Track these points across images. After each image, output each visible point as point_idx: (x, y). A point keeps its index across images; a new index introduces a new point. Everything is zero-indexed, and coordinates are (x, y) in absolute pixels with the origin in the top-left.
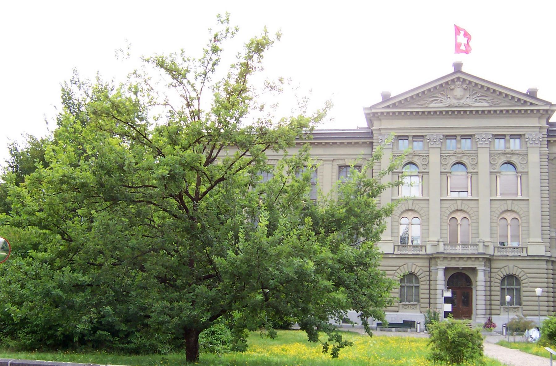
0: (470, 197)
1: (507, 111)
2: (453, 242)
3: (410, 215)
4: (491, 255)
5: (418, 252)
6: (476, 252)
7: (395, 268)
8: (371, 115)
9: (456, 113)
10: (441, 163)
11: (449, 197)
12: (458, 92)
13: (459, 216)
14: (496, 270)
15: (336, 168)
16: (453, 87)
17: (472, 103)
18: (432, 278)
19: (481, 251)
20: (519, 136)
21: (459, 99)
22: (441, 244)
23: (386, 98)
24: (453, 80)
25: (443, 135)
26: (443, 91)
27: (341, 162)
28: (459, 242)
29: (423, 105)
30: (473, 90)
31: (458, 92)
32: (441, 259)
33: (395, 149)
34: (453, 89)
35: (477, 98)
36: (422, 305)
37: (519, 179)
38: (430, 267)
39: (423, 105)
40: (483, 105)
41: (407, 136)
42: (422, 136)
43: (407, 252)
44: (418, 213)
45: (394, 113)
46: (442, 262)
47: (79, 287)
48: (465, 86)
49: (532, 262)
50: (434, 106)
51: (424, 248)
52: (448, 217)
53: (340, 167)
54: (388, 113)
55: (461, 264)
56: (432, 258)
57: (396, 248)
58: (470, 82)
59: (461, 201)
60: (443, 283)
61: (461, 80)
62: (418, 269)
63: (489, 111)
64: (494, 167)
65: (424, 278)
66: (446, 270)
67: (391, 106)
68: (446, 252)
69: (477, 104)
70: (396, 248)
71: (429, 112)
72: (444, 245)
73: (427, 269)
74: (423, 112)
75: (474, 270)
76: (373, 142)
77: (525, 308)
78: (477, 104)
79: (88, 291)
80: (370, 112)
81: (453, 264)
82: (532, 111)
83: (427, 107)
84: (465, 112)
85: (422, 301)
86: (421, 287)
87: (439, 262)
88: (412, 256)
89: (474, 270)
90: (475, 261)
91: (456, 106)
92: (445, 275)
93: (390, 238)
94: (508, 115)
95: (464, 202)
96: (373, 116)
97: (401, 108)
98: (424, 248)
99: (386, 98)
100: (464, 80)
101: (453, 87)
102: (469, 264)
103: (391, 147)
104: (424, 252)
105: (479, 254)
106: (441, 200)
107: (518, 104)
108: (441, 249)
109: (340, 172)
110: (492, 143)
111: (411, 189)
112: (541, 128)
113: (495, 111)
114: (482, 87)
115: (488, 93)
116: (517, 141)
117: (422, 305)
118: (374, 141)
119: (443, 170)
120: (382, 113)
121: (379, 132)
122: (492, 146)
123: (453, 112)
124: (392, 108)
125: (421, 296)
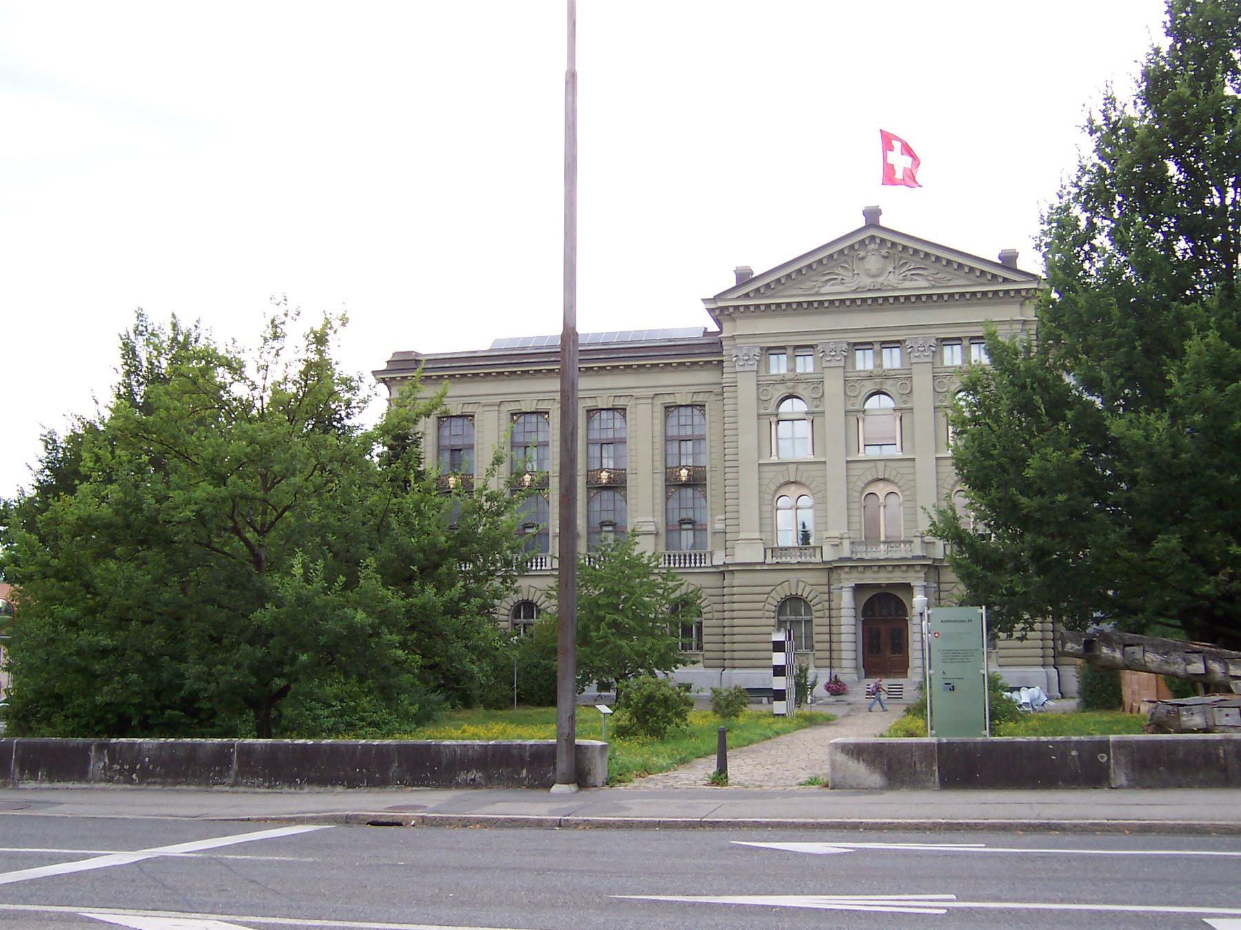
0: (899, 455)
1: (962, 295)
2: (871, 538)
3: (793, 491)
4: (935, 560)
5: (808, 559)
6: (909, 555)
7: (768, 589)
8: (717, 312)
9: (869, 302)
10: (758, 398)
11: (861, 456)
12: (873, 262)
13: (881, 490)
14: (949, 586)
15: (659, 411)
16: (862, 254)
17: (897, 282)
18: (834, 605)
19: (918, 553)
20: (898, 343)
21: (874, 276)
22: (846, 543)
23: (744, 277)
24: (862, 242)
25: (849, 344)
26: (846, 262)
27: (668, 400)
28: (883, 538)
29: (810, 289)
30: (901, 258)
31: (873, 262)
32: (847, 570)
33: (763, 372)
34: (863, 258)
35: (909, 273)
36: (818, 654)
37: (898, 421)
38: (829, 585)
39: (810, 289)
40: (919, 285)
41: (784, 348)
42: (811, 346)
43: (789, 559)
44: (808, 487)
45: (757, 306)
46: (848, 576)
47: (104, 652)
48: (884, 252)
49: (750, 575)
50: (831, 291)
51: (818, 551)
52: (861, 493)
53: (668, 408)
54: (747, 307)
55: (883, 578)
56: (832, 569)
57: (769, 552)
58: (894, 244)
59: (794, 466)
60: (852, 612)
61: (878, 241)
62: (808, 589)
63: (929, 296)
64: (941, 397)
65: (819, 606)
66: (858, 589)
67: (752, 295)
68: (855, 557)
69: (907, 284)
70: (769, 552)
71: (821, 303)
72: (852, 543)
73: (825, 589)
74: (810, 303)
75: (908, 588)
76: (722, 361)
77: (1002, 652)
78: (907, 284)
79: (112, 658)
80: (714, 306)
81: (869, 578)
82: (1007, 292)
83: (817, 294)
84: (886, 299)
85: (817, 646)
86: (815, 621)
87: (843, 576)
88: (797, 567)
89: (908, 588)
90: (907, 571)
91: (879, 290)
92: (855, 598)
93: (757, 535)
94: (963, 302)
95: (889, 464)
96: (721, 310)
97: (768, 297)
98: (818, 551)
99: (744, 277)
100: (883, 240)
101: (862, 254)
102: (897, 578)
103: (755, 368)
104: (818, 559)
105: (914, 558)
106: (848, 462)
107: (982, 280)
108: (846, 551)
109: (666, 417)
110: (938, 355)
111: (794, 440)
112: (1024, 322)
113: (940, 296)
114: (916, 251)
115: (927, 262)
116: (896, 352)
117: (818, 654)
118: (724, 359)
119: (850, 408)
120: (736, 308)
121: (731, 342)
122: (937, 360)
123: (864, 300)
124: (754, 298)
125: (816, 638)
